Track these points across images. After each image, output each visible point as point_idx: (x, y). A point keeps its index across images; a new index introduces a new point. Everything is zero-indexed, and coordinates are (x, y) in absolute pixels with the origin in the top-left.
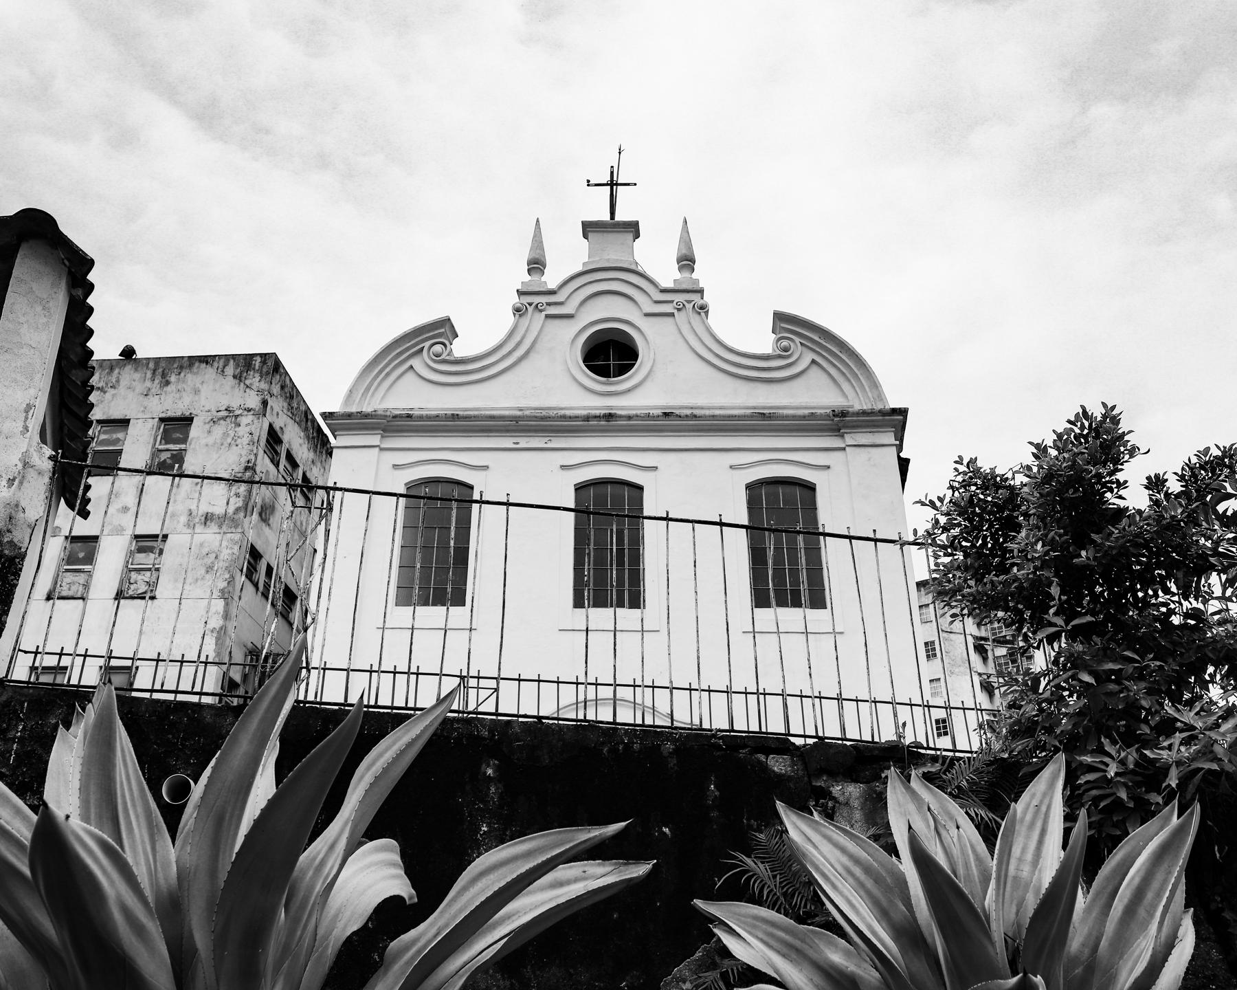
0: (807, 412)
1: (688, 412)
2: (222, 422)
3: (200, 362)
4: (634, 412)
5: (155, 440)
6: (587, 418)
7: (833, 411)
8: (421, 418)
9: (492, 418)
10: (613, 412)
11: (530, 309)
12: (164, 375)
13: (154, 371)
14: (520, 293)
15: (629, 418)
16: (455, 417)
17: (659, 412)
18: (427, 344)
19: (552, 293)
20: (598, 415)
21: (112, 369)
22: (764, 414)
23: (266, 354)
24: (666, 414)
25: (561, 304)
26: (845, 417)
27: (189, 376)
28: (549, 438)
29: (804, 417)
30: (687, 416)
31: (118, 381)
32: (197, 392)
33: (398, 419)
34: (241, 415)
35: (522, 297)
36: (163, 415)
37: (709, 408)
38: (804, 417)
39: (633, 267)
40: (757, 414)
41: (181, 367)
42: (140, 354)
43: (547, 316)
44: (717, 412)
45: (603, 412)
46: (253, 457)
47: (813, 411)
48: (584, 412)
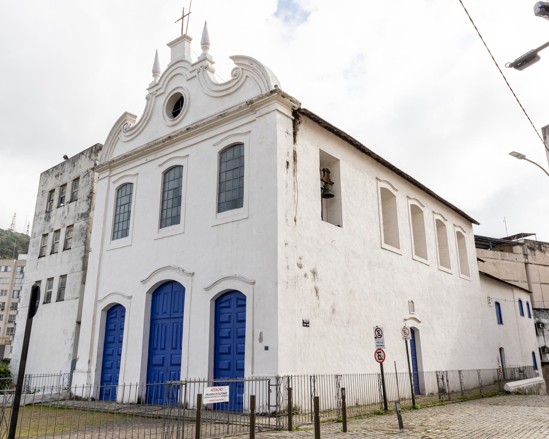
0: (238, 107)
1: (194, 125)
2: (86, 176)
3: (82, 154)
4: (177, 133)
5: (72, 189)
6: (163, 141)
7: (247, 102)
8: (117, 160)
9: (136, 153)
10: (170, 135)
11: (151, 96)
12: (74, 163)
13: (72, 162)
14: (148, 89)
15: (176, 136)
16: (125, 156)
17: (185, 129)
18: (122, 126)
19: (157, 85)
20: (166, 138)
21: (64, 165)
22: (221, 115)
23: (96, 145)
24: (187, 129)
25: (161, 88)
26: (253, 103)
27: (79, 161)
28: (156, 154)
29: (237, 110)
30: (195, 127)
31: (65, 170)
32: (81, 166)
33: (111, 163)
34: (90, 172)
35: (150, 90)
36: (74, 179)
37: (207, 118)
38: (237, 110)
39: (183, 59)
40: (219, 116)
41: (78, 158)
42: (69, 157)
43: (156, 97)
44: (205, 121)
45: (167, 137)
46: (92, 188)
47: (240, 106)
48: (161, 139)
